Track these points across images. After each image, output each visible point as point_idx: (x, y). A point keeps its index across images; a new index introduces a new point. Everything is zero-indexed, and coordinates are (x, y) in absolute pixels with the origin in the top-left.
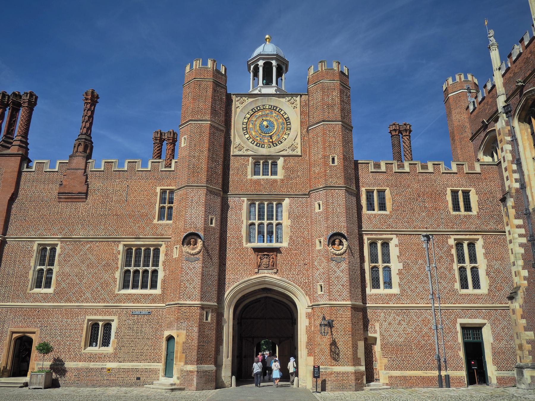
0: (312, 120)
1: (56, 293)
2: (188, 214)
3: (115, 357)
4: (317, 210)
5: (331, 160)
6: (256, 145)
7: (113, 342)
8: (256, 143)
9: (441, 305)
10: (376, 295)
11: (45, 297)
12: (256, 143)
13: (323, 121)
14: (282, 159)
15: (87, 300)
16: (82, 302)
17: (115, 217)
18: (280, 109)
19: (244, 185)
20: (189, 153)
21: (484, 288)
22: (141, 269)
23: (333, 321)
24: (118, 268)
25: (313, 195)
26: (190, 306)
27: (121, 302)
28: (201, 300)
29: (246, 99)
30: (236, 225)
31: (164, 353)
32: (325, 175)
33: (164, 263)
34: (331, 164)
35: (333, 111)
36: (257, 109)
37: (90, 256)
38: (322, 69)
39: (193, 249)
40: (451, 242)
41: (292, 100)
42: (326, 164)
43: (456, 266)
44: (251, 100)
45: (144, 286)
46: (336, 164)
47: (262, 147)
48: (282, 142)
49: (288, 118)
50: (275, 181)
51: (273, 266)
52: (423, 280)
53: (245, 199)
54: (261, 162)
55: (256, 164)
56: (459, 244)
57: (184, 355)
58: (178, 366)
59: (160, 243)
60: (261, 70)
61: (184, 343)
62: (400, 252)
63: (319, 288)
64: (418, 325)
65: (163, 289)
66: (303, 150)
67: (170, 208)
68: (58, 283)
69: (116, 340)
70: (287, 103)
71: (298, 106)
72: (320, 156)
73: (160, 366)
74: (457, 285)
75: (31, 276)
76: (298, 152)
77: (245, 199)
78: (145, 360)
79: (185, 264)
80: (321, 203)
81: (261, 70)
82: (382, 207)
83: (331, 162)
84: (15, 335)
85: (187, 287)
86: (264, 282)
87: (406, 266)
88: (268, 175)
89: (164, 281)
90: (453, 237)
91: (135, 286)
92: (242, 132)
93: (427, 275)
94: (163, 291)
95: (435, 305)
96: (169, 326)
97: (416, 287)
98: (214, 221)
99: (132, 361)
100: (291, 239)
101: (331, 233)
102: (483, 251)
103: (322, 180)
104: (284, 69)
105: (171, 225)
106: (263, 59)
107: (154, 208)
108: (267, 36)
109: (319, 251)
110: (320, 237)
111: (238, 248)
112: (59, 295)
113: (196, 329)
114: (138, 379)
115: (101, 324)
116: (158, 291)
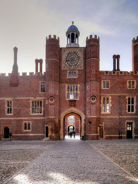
3: (32, 132)
4: (88, 89)
11: (11, 116)
15: (22, 117)
21: (134, 112)
31: (45, 131)
39: (52, 101)
40: (127, 98)
43: (127, 105)
51: (75, 106)
56: (129, 99)
65: (44, 113)
72: (89, 71)
73: (45, 135)
74: (127, 111)
75: (6, 110)
77: (66, 85)
79: (50, 106)
84: (4, 127)
90: (127, 96)
92: (65, 62)
96: (47, 124)
98: (57, 92)
104: (78, 35)
106: (71, 32)
112: (14, 116)
116: (42, 114)
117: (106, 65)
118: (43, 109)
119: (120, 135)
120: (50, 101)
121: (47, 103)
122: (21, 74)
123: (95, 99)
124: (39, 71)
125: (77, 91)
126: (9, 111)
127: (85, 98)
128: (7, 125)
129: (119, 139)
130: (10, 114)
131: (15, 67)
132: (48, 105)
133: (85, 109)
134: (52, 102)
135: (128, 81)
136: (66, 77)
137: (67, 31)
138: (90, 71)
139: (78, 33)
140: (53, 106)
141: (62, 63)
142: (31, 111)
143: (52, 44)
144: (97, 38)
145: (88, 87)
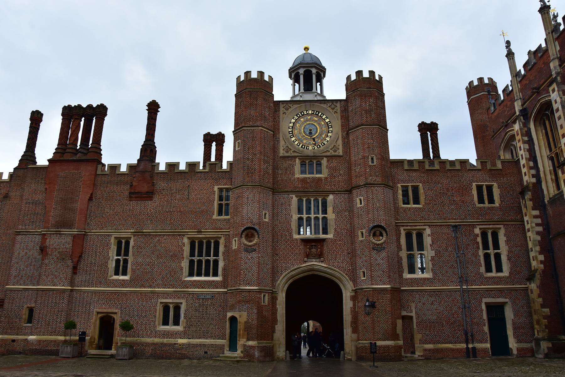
0: (351, 124)
1: (132, 279)
2: (245, 211)
4: (359, 205)
5: (370, 159)
6: (302, 147)
7: (183, 321)
9: (469, 287)
10: (411, 279)
11: (123, 284)
13: (363, 125)
14: (325, 159)
16: (155, 287)
17: (179, 214)
19: (292, 183)
20: (244, 156)
22: (204, 258)
23: (375, 302)
24: (183, 258)
25: (354, 192)
26: (250, 291)
27: (188, 288)
28: (258, 285)
30: (286, 219)
31: (228, 331)
32: (365, 174)
33: (224, 253)
34: (370, 164)
35: (371, 116)
37: (159, 248)
39: (250, 241)
40: (477, 231)
41: (333, 106)
43: (481, 253)
44: (296, 106)
45: (207, 275)
46: (375, 163)
48: (324, 144)
50: (320, 179)
51: (320, 256)
52: (452, 265)
53: (294, 196)
54: (307, 162)
55: (303, 164)
57: (246, 333)
58: (241, 342)
59: (220, 236)
60: (302, 77)
61: (245, 322)
62: (432, 241)
63: (362, 274)
64: (449, 305)
65: (225, 276)
66: (345, 152)
67: (227, 205)
68: (133, 271)
69: (185, 320)
70: (329, 109)
71: (339, 111)
73: (224, 342)
75: (112, 265)
76: (340, 152)
78: (211, 337)
79: (243, 254)
80: (362, 198)
81: (302, 77)
82: (416, 201)
83: (370, 162)
84: (100, 315)
85: (246, 275)
86: (313, 270)
87: (438, 253)
88: (313, 174)
89: (224, 269)
90: (478, 227)
91: (199, 275)
93: (456, 261)
94: (224, 278)
95: (464, 287)
96: (232, 308)
97: (447, 272)
98: (267, 215)
99: (200, 338)
100: (336, 231)
101: (372, 225)
102: (505, 239)
103: (363, 178)
105: (229, 220)
106: (304, 67)
107: (213, 205)
109: (361, 241)
110: (362, 229)
111: (288, 240)
112: (132, 282)
113: (255, 311)
114: (206, 353)
115: (171, 306)
116: (218, 279)
117: (404, 145)
118: (221, 264)
119: (470, 346)
120: (246, 239)
121: (234, 246)
122: (162, 168)
123: (385, 236)
124: (213, 159)
125: (326, 214)
126: (121, 268)
127: (352, 234)
128: (110, 310)
129: (468, 357)
130: (122, 278)
131: (149, 149)
132: (237, 251)
133: (353, 264)
134: (250, 244)
135: (474, 184)
136: (293, 174)
137: (291, 65)
138: (364, 157)
139: (322, 71)
140: (254, 254)
141: (281, 138)
142: (186, 270)
143: (252, 91)
144: (377, 78)
145: (358, 201)
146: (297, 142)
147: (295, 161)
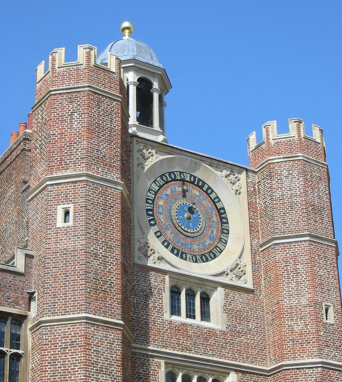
5: (324, 311)
8: (171, 247)
12: (171, 247)
14: (220, 290)
18: (209, 188)
20: (87, 246)
29: (154, 151)
32: (318, 340)
36: (170, 176)
38: (299, 135)
41: (232, 177)
42: (318, 320)
47: (182, 257)
49: (223, 209)
50: (211, 332)
55: (175, 293)
71: (244, 190)
72: (304, 301)
83: (325, 317)
108: (126, 24)
136: (160, 311)
141: (136, 222)
146: (163, 238)
147: (163, 281)
